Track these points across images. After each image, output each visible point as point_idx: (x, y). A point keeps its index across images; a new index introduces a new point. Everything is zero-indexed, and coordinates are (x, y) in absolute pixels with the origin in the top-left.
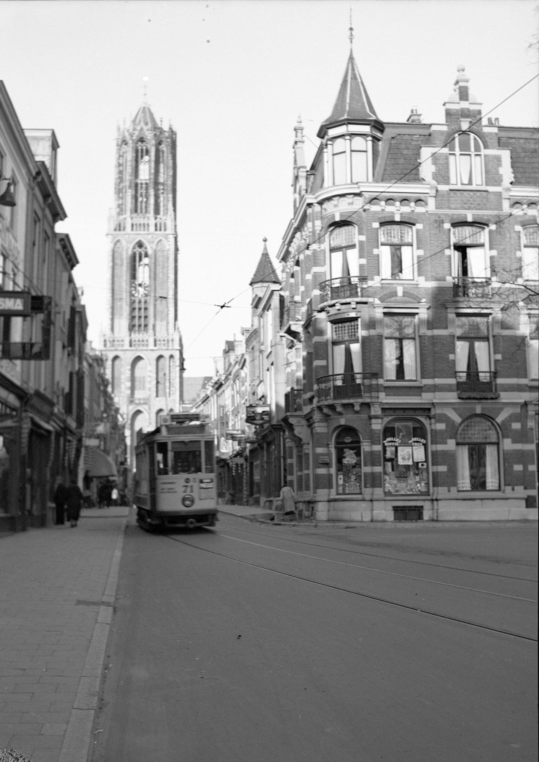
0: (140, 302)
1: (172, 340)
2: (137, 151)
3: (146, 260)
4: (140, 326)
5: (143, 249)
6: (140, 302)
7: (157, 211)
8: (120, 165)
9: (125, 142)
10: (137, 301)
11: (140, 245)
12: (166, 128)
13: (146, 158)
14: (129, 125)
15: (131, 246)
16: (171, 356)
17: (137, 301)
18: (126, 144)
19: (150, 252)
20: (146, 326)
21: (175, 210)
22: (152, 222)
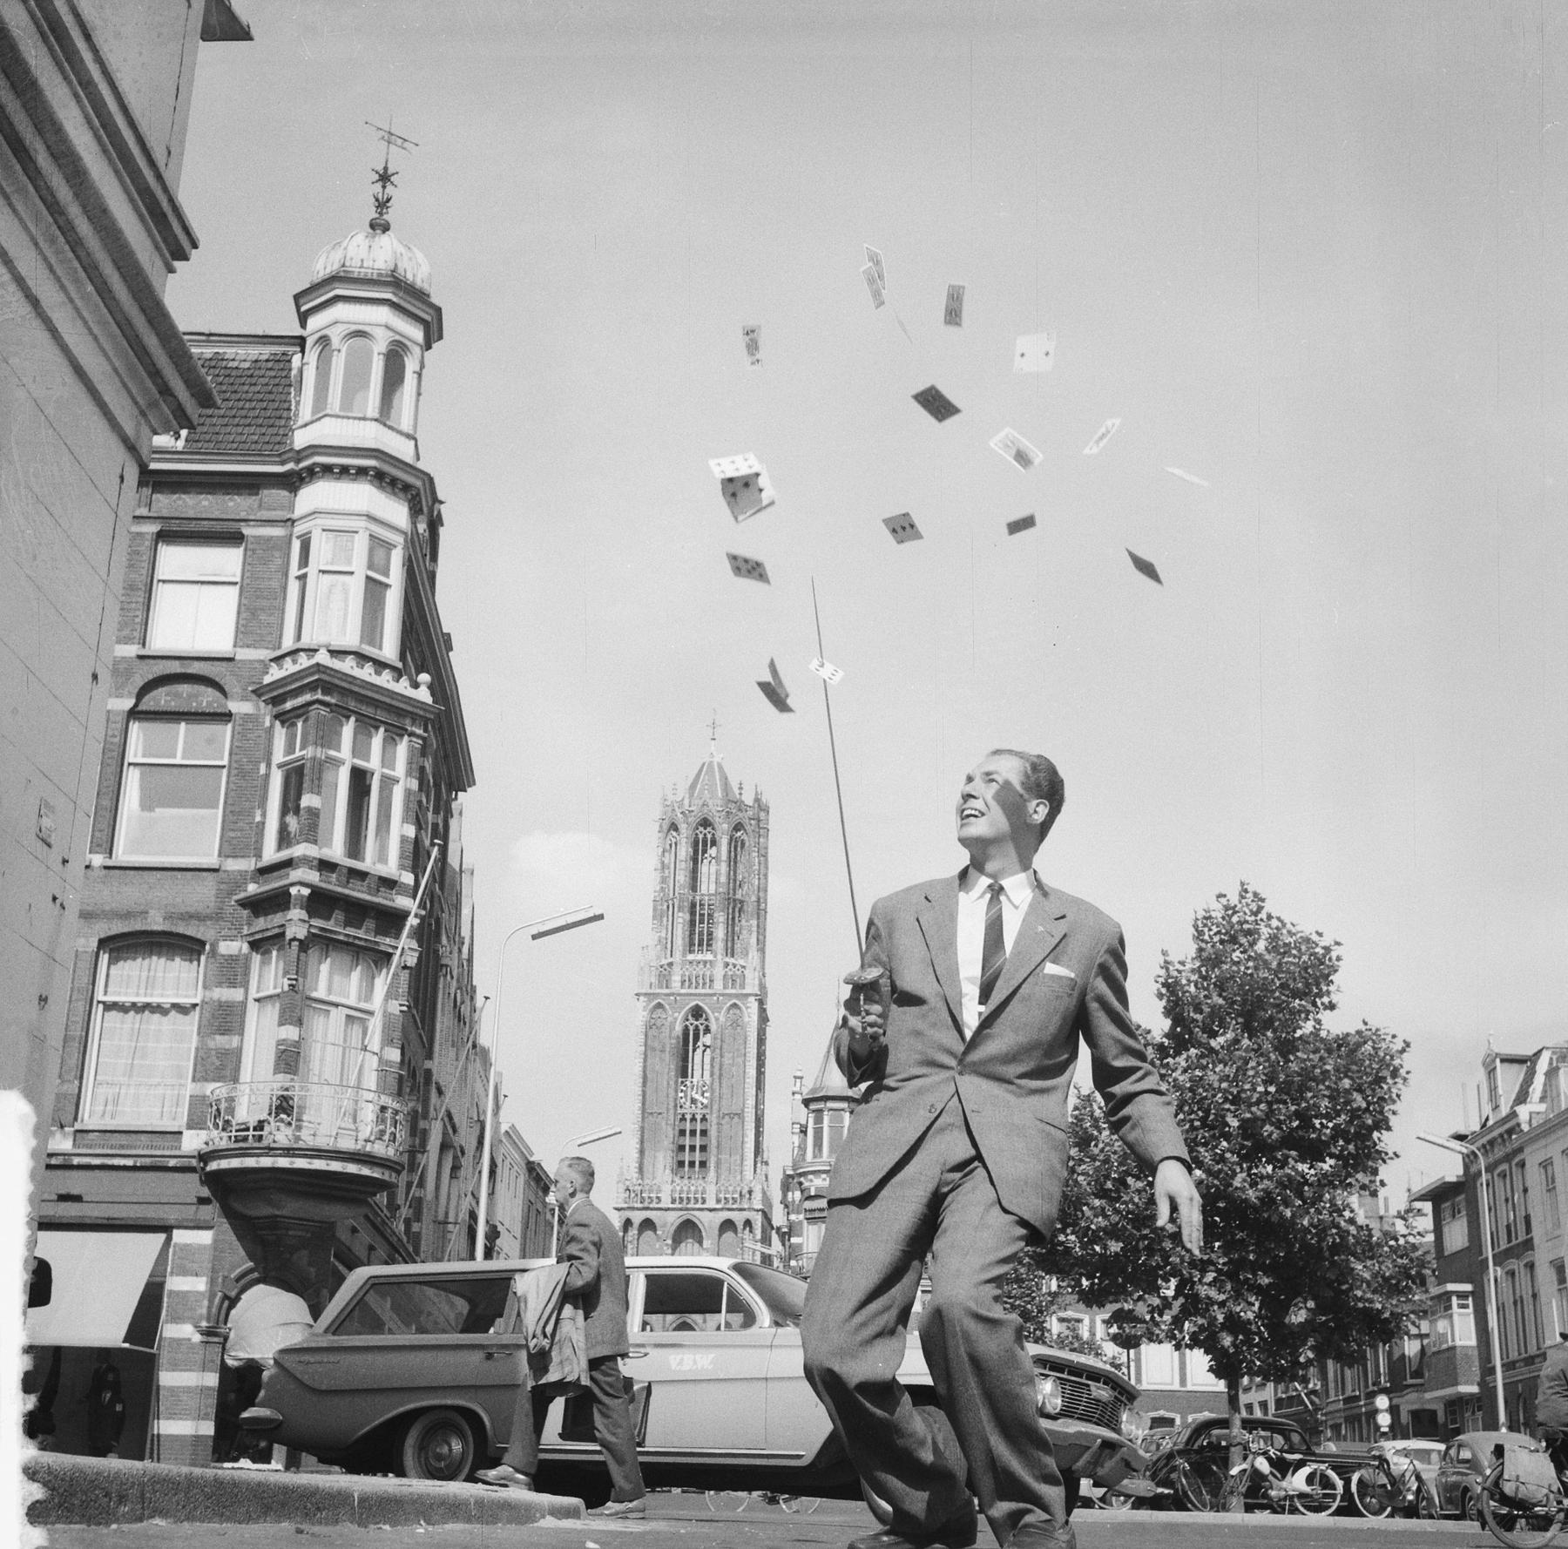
0: (693, 1119)
1: (750, 1192)
2: (696, 843)
3: (706, 1039)
4: (692, 1164)
5: (702, 1021)
6: (693, 1119)
7: (730, 951)
8: (664, 866)
9: (674, 827)
10: (688, 1117)
11: (697, 1012)
12: (748, 799)
13: (713, 851)
14: (682, 793)
15: (680, 1017)
16: (748, 1223)
17: (688, 1117)
18: (676, 829)
19: (713, 1027)
20: (703, 1164)
21: (762, 950)
22: (719, 972)
